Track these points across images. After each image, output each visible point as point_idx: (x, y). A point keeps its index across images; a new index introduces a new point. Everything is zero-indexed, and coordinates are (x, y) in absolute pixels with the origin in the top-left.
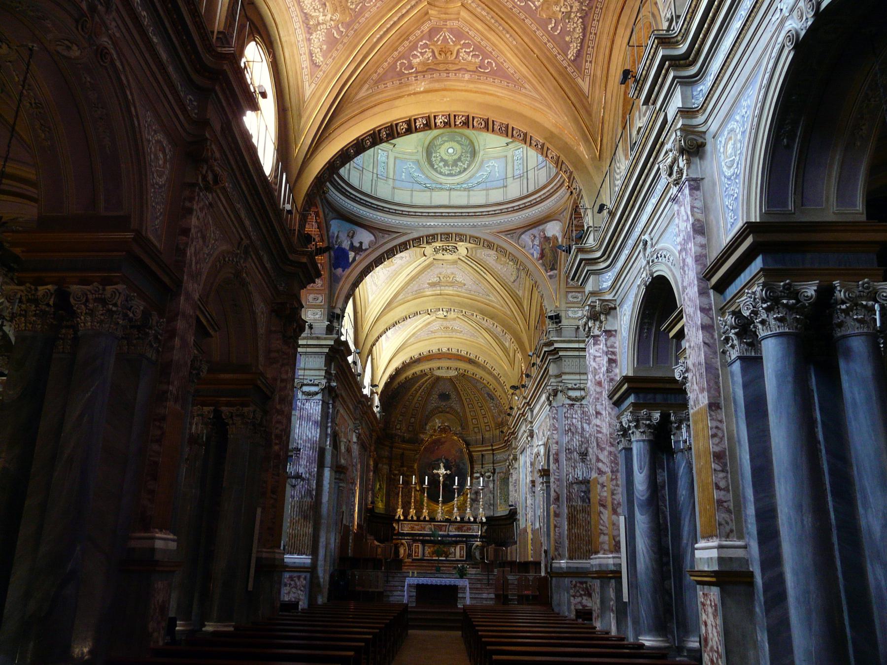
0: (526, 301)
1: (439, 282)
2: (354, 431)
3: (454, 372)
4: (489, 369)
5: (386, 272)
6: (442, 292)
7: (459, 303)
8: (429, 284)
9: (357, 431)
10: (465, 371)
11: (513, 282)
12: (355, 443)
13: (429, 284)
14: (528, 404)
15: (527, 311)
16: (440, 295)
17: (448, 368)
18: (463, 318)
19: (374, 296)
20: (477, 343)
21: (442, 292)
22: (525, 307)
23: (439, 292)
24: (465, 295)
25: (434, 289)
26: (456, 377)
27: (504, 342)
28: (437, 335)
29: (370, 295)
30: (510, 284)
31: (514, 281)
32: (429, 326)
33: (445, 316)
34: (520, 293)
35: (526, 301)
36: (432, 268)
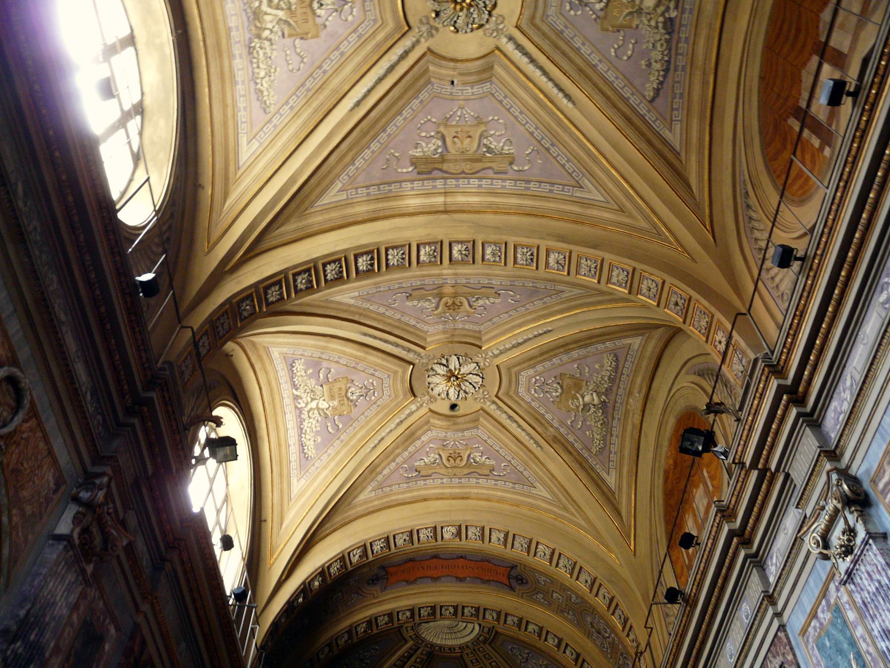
0: (693, 158)
1: (443, 159)
2: (76, 499)
3: (470, 626)
4: (564, 588)
5: (295, 60)
6: (450, 199)
7: (497, 228)
8: (414, 162)
9: (84, 495)
10: (499, 613)
11: (652, 101)
12: (59, 538)
13: (414, 162)
14: (742, 536)
15: (701, 190)
16: (445, 212)
17: (455, 613)
18: (497, 414)
19: (255, 144)
20: (531, 506)
21: (450, 199)
22: (693, 181)
23: (440, 200)
24: (514, 201)
25: (429, 184)
26: (476, 641)
27: (604, 475)
28: (432, 487)
29: (243, 140)
30: (643, 110)
31: (657, 91)
32: (411, 449)
33: (453, 407)
34: (674, 137)
35: (693, 158)
36: (424, 95)
